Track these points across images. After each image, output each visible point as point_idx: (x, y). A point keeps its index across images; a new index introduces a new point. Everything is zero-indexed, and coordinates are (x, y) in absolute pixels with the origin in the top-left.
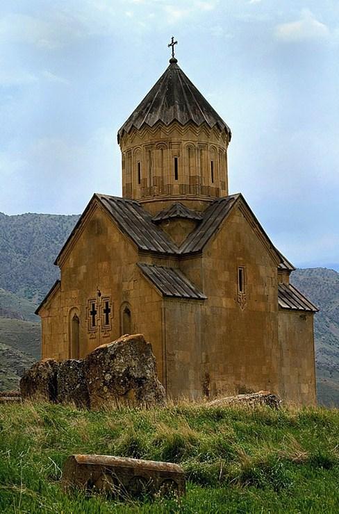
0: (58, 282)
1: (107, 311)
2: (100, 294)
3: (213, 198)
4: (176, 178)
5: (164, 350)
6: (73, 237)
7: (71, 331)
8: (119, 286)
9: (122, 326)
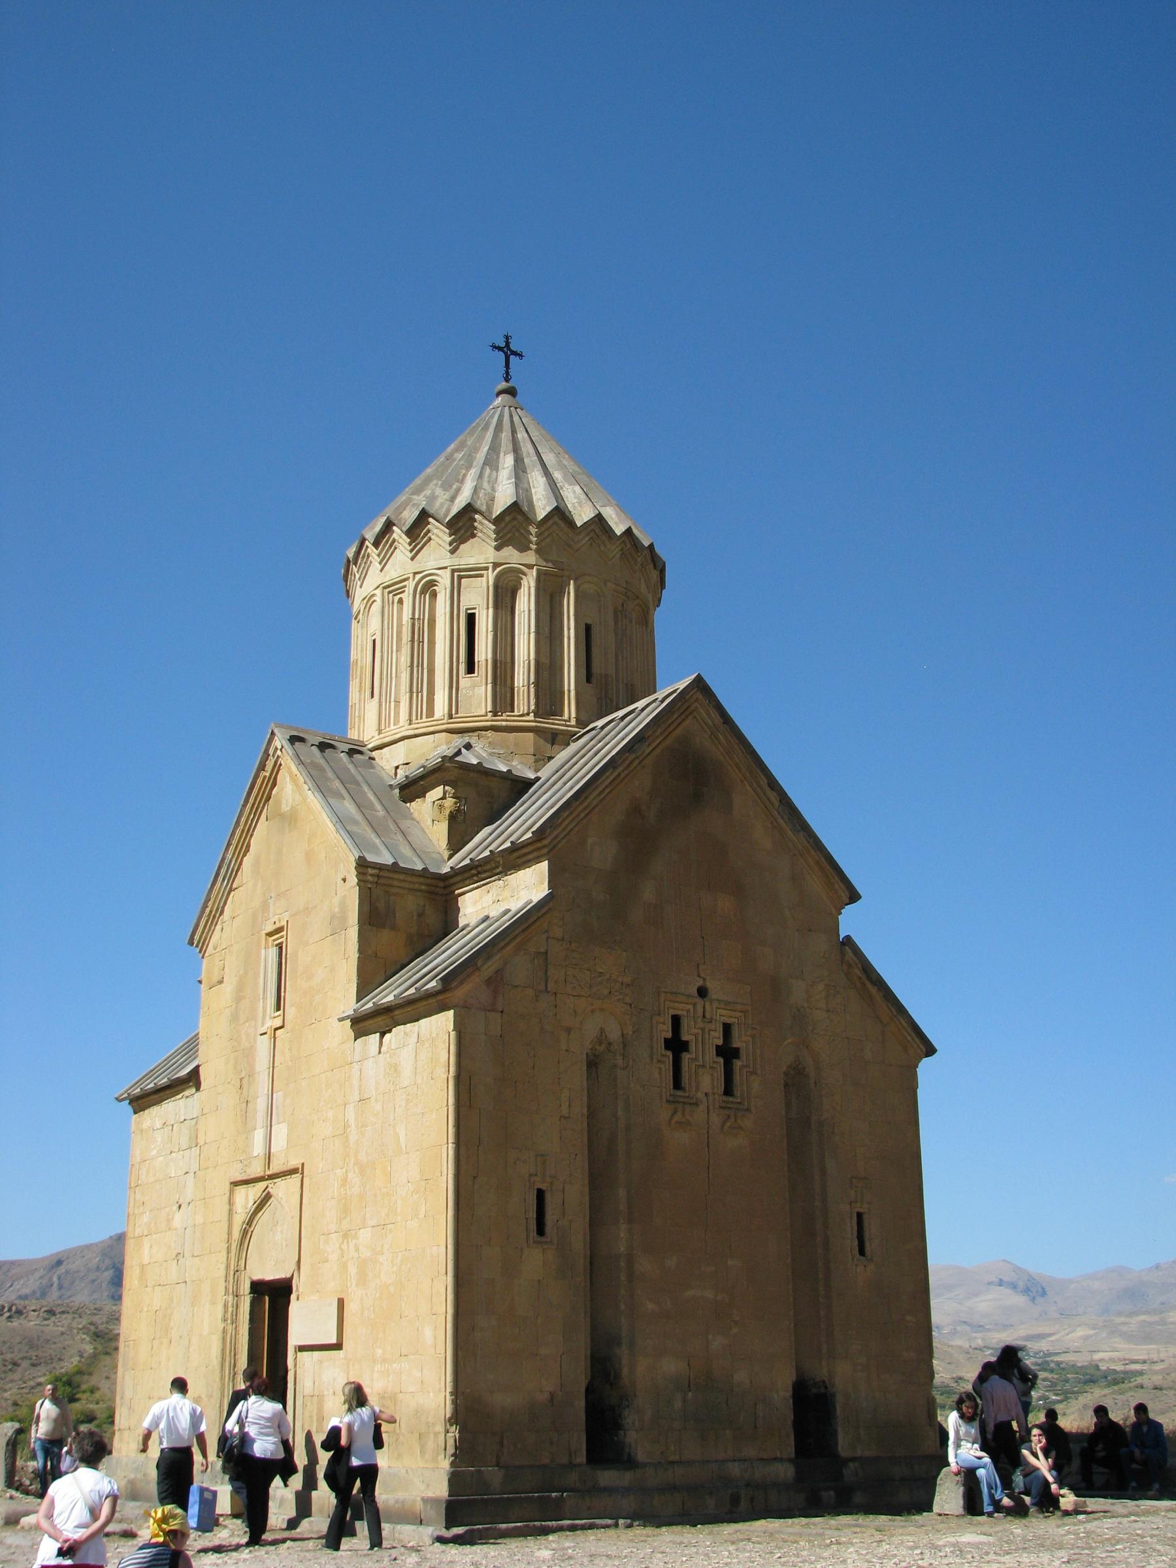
1: (728, 1053)
2: (702, 992)
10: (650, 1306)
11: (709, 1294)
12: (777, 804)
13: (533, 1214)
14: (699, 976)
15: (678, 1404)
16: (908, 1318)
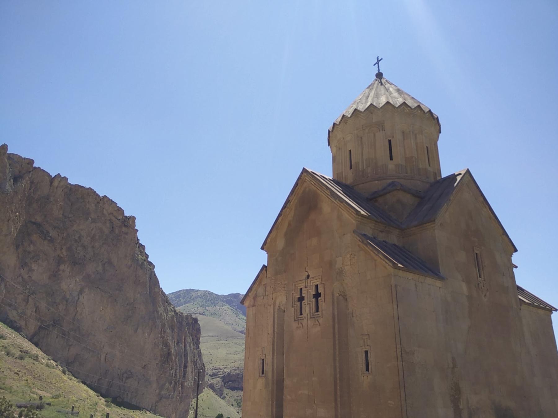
0: (264, 266)
3: (432, 180)
4: (391, 159)
5: (399, 346)
6: (280, 218)
7: (276, 321)
8: (331, 264)
9: (336, 313)
10: (289, 397)
13: (261, 368)
14: (306, 271)
16: (389, 402)
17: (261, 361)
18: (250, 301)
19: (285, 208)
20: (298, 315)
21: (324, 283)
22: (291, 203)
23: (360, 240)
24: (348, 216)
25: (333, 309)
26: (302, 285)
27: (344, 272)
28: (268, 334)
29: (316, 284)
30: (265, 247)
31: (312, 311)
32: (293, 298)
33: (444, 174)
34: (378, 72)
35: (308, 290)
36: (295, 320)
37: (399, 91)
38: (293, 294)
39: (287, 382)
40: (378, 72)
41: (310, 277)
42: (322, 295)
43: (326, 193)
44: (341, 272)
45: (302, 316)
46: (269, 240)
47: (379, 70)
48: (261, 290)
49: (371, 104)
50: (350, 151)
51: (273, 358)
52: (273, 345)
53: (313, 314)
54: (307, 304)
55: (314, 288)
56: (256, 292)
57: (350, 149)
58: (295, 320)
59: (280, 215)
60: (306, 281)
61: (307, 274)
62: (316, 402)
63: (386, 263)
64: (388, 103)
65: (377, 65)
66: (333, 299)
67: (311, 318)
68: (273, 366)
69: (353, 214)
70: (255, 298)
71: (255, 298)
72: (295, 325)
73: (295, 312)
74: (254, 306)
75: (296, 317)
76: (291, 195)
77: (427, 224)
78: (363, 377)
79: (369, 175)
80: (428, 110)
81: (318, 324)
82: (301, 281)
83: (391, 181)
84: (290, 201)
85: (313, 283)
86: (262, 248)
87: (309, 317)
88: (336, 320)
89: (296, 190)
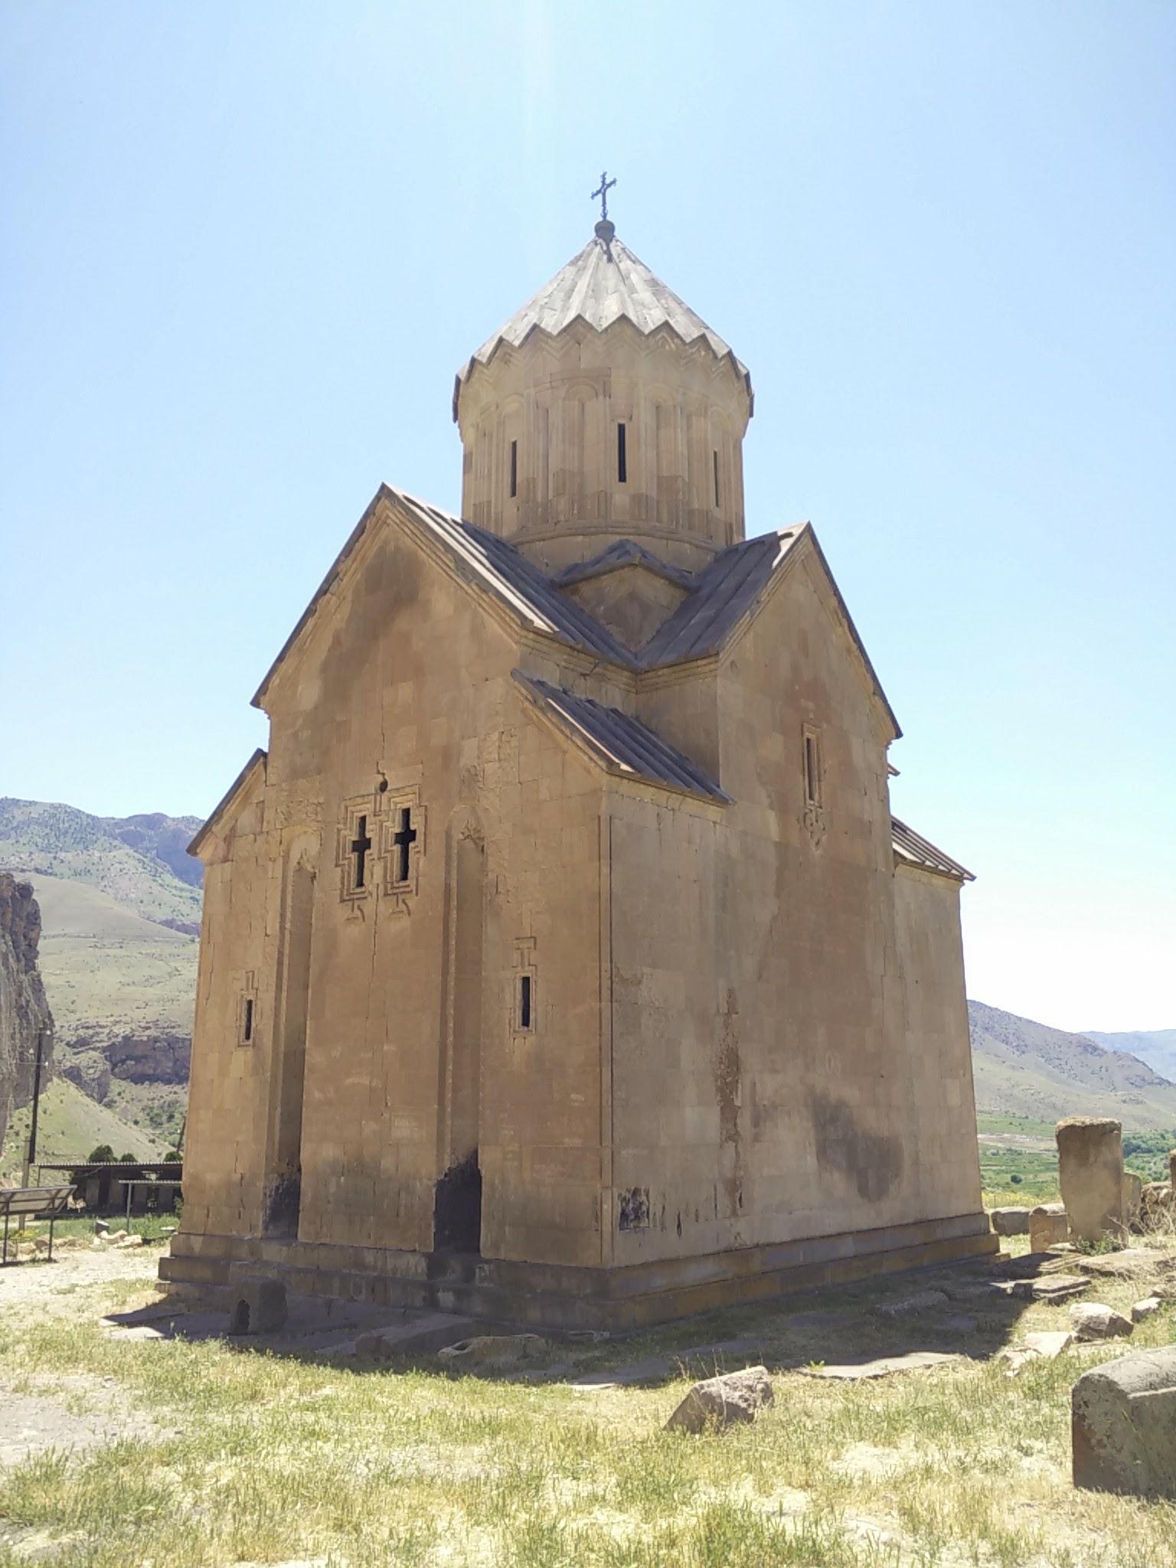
0: (260, 754)
1: (406, 837)
3: (720, 544)
4: (622, 478)
5: (606, 965)
6: (311, 622)
7: (289, 902)
8: (448, 755)
9: (454, 884)
10: (317, 1095)
11: (365, 1081)
12: (452, 565)
13: (244, 1023)
14: (379, 772)
15: (332, 1189)
16: (573, 1096)
17: (245, 1006)
18: (216, 848)
19: (325, 593)
20: (352, 886)
21: (427, 804)
22: (342, 580)
23: (529, 697)
24: (500, 631)
25: (448, 872)
26: (366, 809)
27: (481, 779)
28: (266, 935)
29: (405, 806)
30: (264, 700)
31: (391, 876)
32: (338, 842)
33: (752, 532)
34: (601, 219)
35: (382, 822)
36: (342, 901)
37: (655, 285)
38: (339, 830)
39: (314, 1057)
40: (601, 219)
41: (389, 788)
42: (420, 836)
43: (443, 561)
44: (472, 779)
45: (363, 889)
46: (276, 680)
47: (605, 216)
48: (247, 818)
49: (579, 317)
50: (514, 444)
51: (278, 999)
52: (280, 963)
53: (392, 883)
54: (379, 859)
55: (399, 817)
56: (234, 822)
57: (513, 440)
58: (342, 901)
59: (310, 612)
60: (378, 797)
61: (380, 779)
62: (389, 1104)
63: (591, 759)
64: (623, 319)
65: (600, 196)
66: (448, 847)
67: (386, 894)
68: (277, 1016)
69: (514, 626)
70: (229, 839)
71: (229, 839)
72: (342, 913)
73: (343, 878)
74: (228, 861)
75: (345, 893)
76: (343, 558)
77: (700, 663)
78: (514, 1039)
79: (562, 518)
80: (725, 351)
81: (406, 912)
82: (363, 796)
83: (618, 538)
84: (341, 575)
85: (396, 804)
86: (255, 703)
87: (381, 892)
88: (454, 903)
89: (358, 546)
